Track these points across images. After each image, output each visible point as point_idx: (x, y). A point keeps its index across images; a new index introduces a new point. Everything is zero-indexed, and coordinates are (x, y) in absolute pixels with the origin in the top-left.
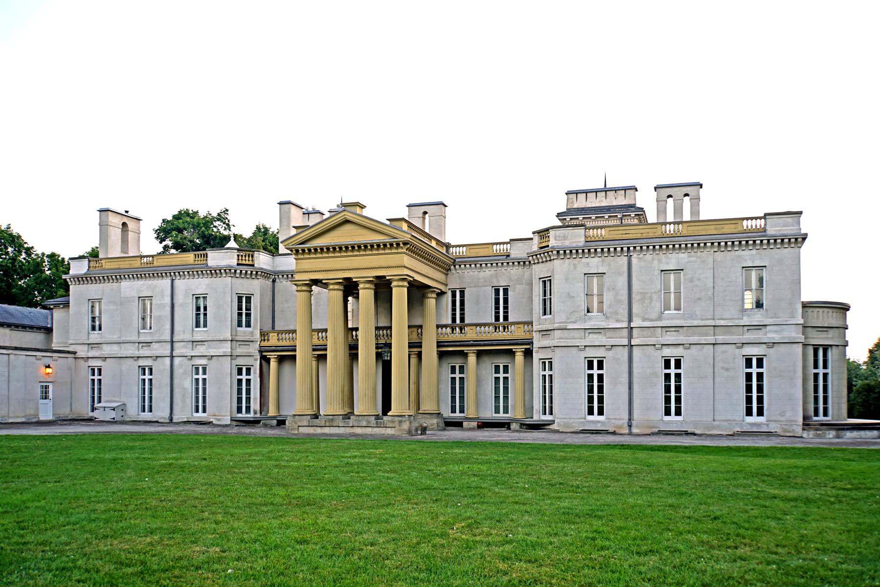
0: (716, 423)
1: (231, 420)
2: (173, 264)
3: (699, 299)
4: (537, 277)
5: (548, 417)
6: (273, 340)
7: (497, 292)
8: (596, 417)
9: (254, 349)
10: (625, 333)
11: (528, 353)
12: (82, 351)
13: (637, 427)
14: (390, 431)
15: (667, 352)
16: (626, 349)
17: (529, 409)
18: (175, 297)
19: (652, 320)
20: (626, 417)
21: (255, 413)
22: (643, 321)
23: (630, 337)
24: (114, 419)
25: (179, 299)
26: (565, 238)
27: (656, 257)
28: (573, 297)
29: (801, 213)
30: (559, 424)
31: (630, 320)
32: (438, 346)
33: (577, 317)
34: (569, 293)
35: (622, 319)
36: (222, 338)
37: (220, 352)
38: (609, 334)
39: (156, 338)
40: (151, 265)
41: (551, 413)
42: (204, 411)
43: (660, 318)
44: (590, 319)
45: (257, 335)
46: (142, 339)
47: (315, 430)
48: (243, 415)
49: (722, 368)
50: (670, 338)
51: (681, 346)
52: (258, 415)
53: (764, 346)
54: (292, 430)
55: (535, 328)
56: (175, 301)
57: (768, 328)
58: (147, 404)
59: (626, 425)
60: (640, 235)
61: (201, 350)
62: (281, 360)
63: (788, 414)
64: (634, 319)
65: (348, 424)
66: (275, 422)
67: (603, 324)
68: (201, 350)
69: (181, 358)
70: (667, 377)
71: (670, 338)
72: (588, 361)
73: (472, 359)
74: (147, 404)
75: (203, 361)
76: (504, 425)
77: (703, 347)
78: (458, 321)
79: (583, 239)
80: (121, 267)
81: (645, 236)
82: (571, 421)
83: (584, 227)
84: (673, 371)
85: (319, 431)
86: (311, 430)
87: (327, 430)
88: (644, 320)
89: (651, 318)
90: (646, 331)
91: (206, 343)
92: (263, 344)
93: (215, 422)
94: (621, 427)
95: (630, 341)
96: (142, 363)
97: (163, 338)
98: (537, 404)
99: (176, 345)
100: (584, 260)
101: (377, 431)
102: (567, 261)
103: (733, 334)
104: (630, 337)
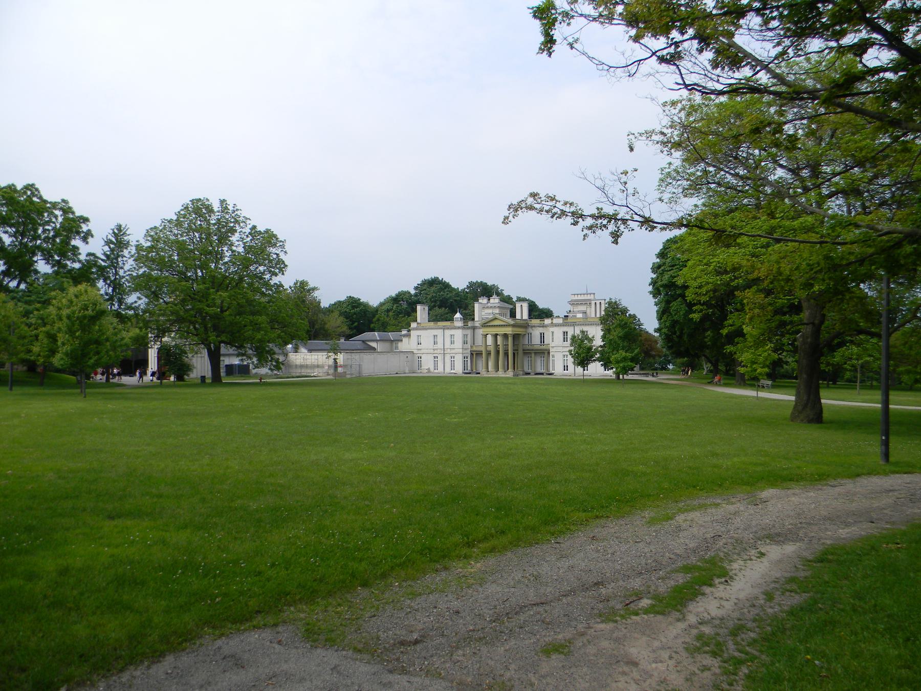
5: (553, 372)
6: (474, 349)
9: (469, 351)
11: (549, 353)
12: (415, 351)
48: (466, 371)
55: (551, 346)
58: (436, 367)
61: (453, 351)
62: (477, 354)
68: (453, 351)
73: (533, 355)
74: (436, 367)
76: (542, 374)
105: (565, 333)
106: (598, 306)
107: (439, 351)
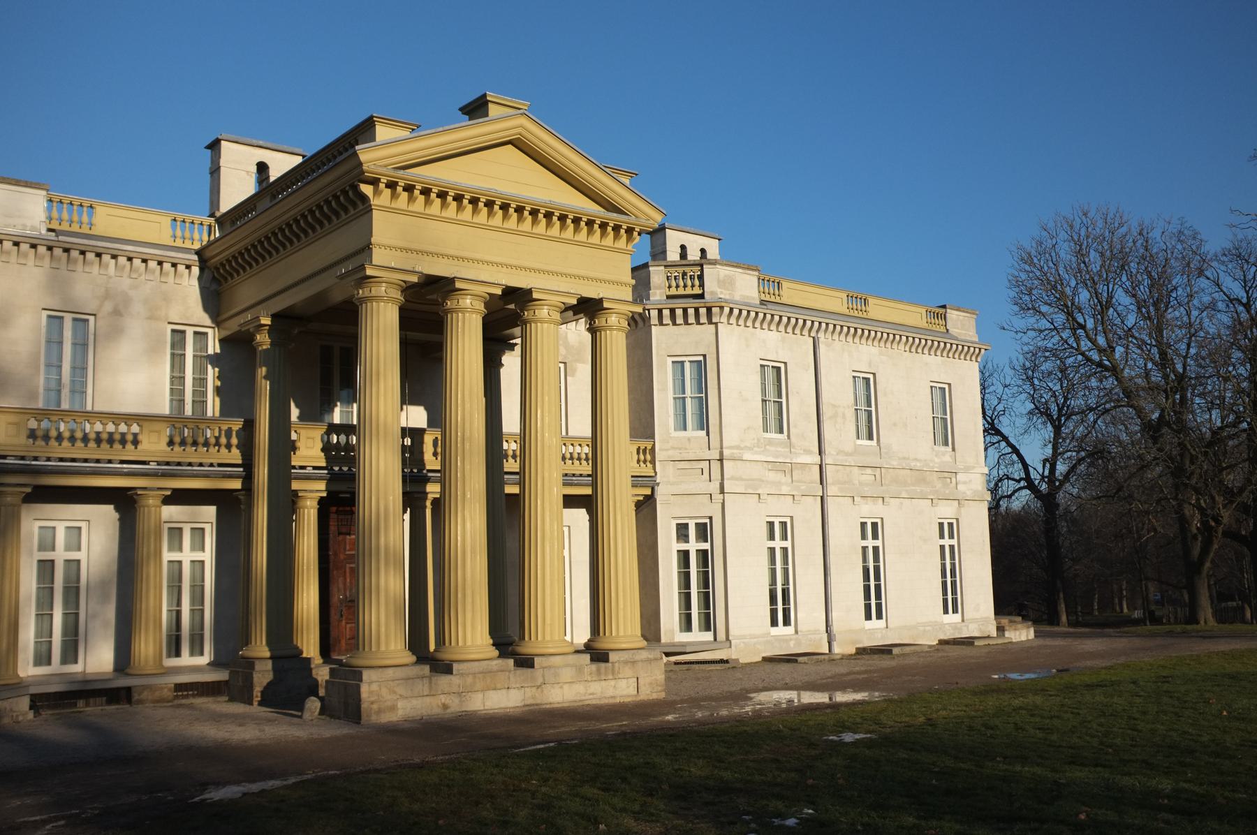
3: (895, 424)
33: (754, 439)
34: (740, 392)
41: (707, 624)
72: (706, 524)
83: (757, 273)
105: (775, 376)
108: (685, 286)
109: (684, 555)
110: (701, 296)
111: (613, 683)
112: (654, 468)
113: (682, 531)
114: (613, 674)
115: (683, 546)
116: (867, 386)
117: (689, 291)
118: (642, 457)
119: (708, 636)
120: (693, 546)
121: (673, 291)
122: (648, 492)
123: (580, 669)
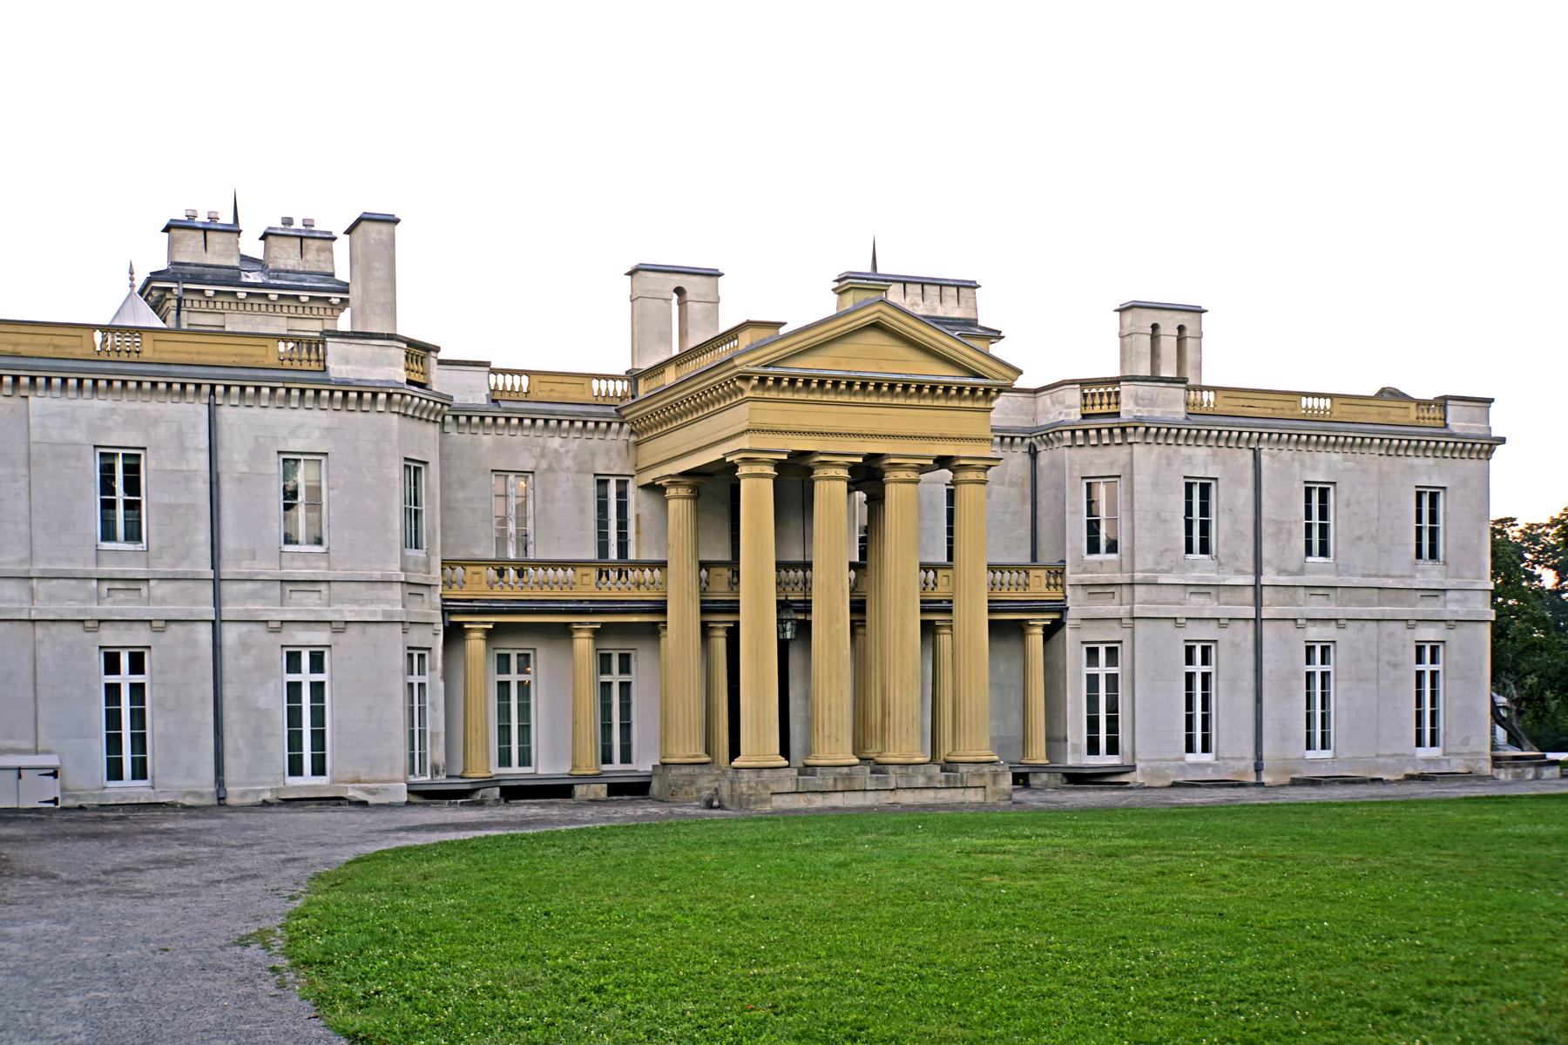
0: (1381, 760)
1: (409, 792)
2: (212, 360)
3: (1359, 538)
4: (1077, 474)
5: (1104, 760)
7: (602, 483)
8: (1198, 757)
9: (430, 607)
10: (1249, 593)
11: (1052, 631)
13: (1270, 773)
14: (973, 796)
15: (1315, 633)
16: (1250, 628)
17: (1055, 740)
18: (223, 456)
19: (1291, 574)
20: (1249, 753)
21: (436, 770)
22: (1278, 574)
23: (1258, 603)
24: (55, 801)
25: (234, 458)
26: (1152, 402)
27: (1297, 455)
28: (1165, 521)
29: (1491, 400)
30: (1144, 774)
31: (1258, 572)
32: (991, 611)
33: (1172, 562)
34: (1158, 514)
35: (1245, 569)
36: (377, 575)
37: (374, 613)
38: (1224, 596)
39: (163, 568)
40: (134, 357)
42: (319, 768)
43: (1301, 571)
44: (1193, 565)
45: (436, 574)
46: (107, 569)
47: (810, 801)
49: (1389, 663)
50: (1318, 607)
51: (1333, 623)
52: (442, 778)
53: (1443, 625)
54: (756, 803)
55: (1071, 578)
56: (222, 467)
57: (1449, 594)
59: (1251, 770)
60: (1270, 411)
61: (307, 605)
63: (1473, 742)
64: (1265, 569)
65: (887, 783)
66: (497, 791)
67: (1215, 578)
68: (307, 605)
69: (245, 628)
70: (113, 691)
71: (1318, 607)
75: (320, 637)
77: (1363, 626)
78: (613, 554)
79: (1182, 409)
80: (22, 350)
81: (1278, 414)
82: (1164, 764)
83: (1183, 385)
84: (125, 679)
85: (818, 802)
86: (800, 802)
87: (836, 800)
88: (1280, 572)
89: (1290, 569)
90: (1283, 593)
91: (323, 587)
92: (451, 594)
93: (371, 800)
94: (1244, 773)
95: (1258, 612)
96: (110, 637)
97: (183, 568)
98: (1077, 733)
99: (228, 589)
100: (1184, 450)
101: (947, 796)
102: (1156, 449)
103: (1401, 602)
104: (1258, 603)
105: (1200, 493)
106: (1168, 344)
107: (164, 600)
108: (1101, 404)
109: (1093, 680)
110: (1117, 414)
111: (962, 790)
112: (1064, 592)
113: (1092, 653)
114: (962, 782)
115: (1093, 670)
116: (1319, 496)
117: (1105, 409)
118: (1052, 581)
119: (1114, 760)
120: (1102, 670)
121: (1089, 410)
122: (1056, 616)
123: (930, 778)
